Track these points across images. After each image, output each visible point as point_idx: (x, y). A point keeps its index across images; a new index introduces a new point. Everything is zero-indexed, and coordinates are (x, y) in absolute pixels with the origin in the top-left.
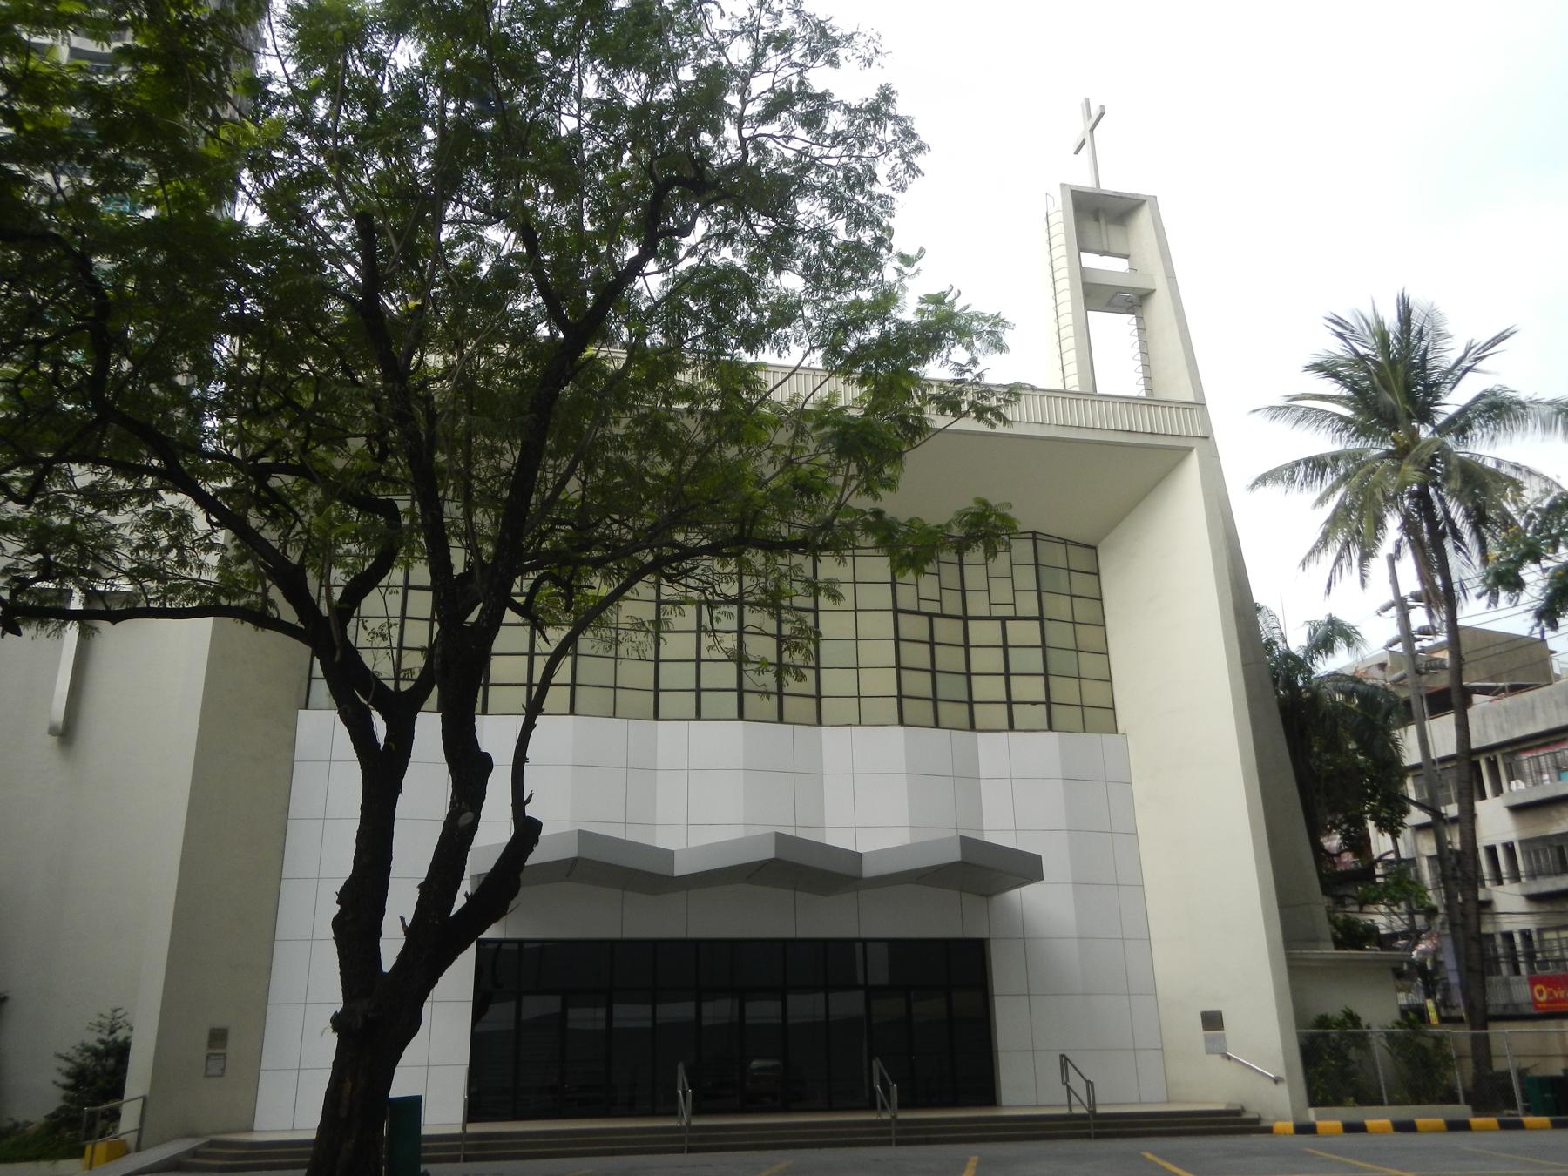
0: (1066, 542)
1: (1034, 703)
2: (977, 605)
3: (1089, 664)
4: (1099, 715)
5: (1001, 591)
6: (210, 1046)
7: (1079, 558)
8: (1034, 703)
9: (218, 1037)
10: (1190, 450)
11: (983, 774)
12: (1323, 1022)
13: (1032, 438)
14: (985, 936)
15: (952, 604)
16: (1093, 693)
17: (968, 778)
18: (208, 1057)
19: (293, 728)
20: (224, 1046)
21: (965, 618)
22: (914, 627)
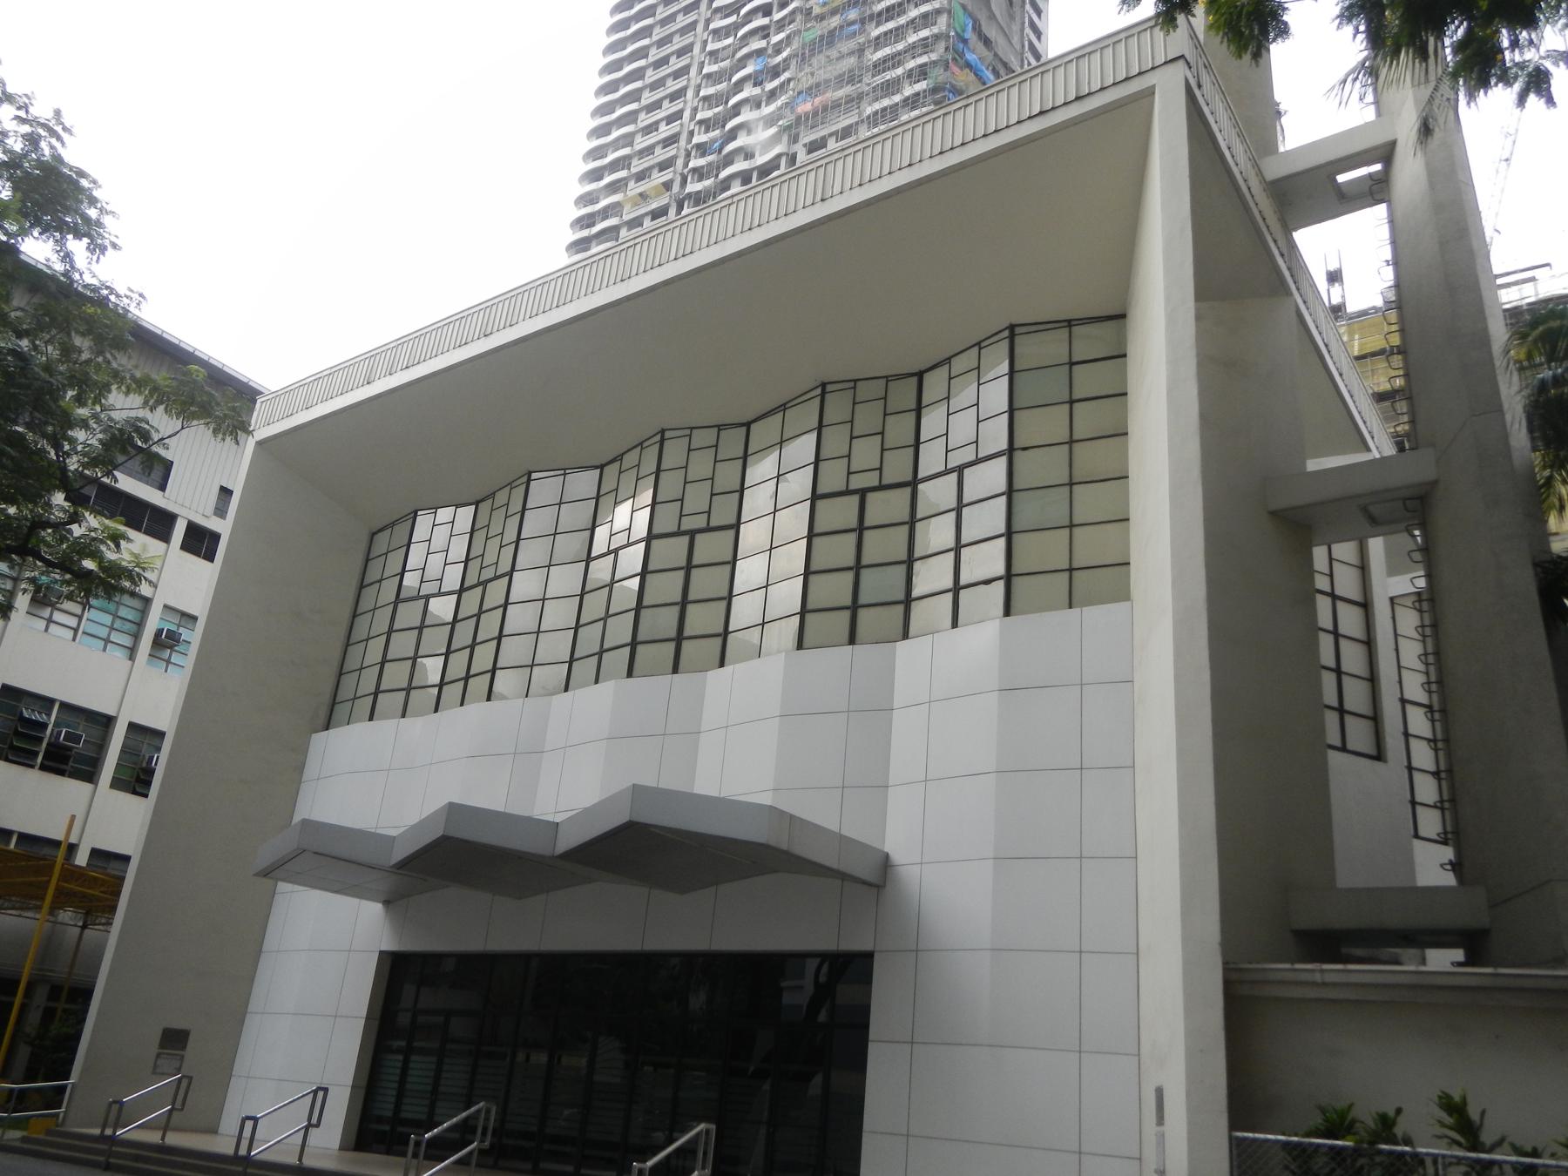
0: (1070, 323)
1: (987, 582)
2: (931, 458)
3: (1089, 502)
4: (1094, 578)
5: (963, 427)
6: (162, 1046)
7: (1088, 342)
8: (987, 582)
9: (174, 1040)
10: (1150, 92)
11: (898, 701)
12: (1337, 1125)
13: (898, 191)
14: (868, 947)
15: (898, 468)
16: (1090, 545)
17: (873, 710)
18: (158, 1056)
19: (301, 751)
20: (184, 1048)
21: (914, 483)
22: (841, 512)
